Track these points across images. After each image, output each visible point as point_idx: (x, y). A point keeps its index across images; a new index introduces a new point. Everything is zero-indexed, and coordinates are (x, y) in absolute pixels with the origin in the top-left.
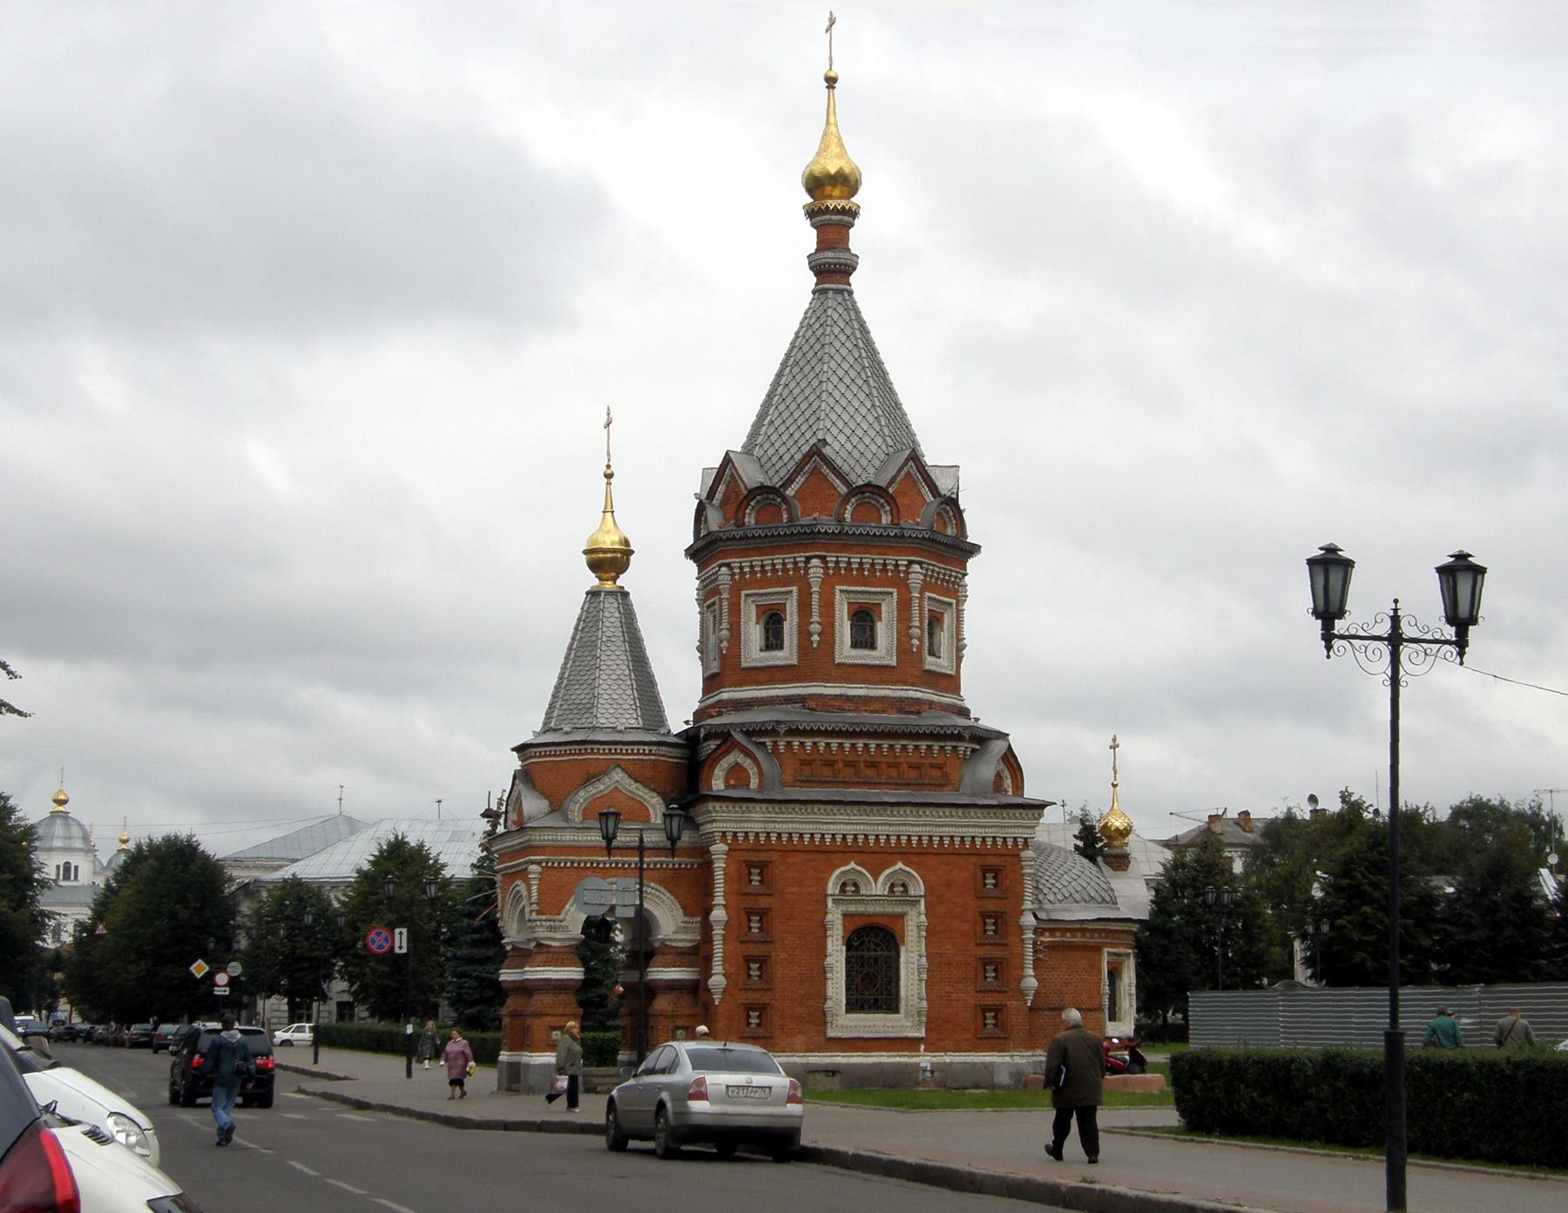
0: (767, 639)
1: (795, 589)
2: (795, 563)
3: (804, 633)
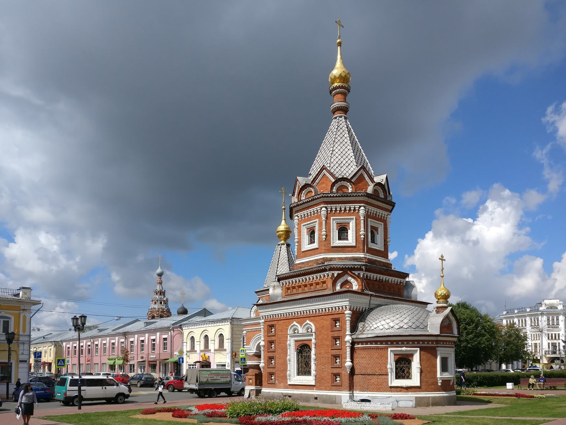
0: (311, 240)
1: (317, 220)
2: (317, 211)
3: (320, 235)
